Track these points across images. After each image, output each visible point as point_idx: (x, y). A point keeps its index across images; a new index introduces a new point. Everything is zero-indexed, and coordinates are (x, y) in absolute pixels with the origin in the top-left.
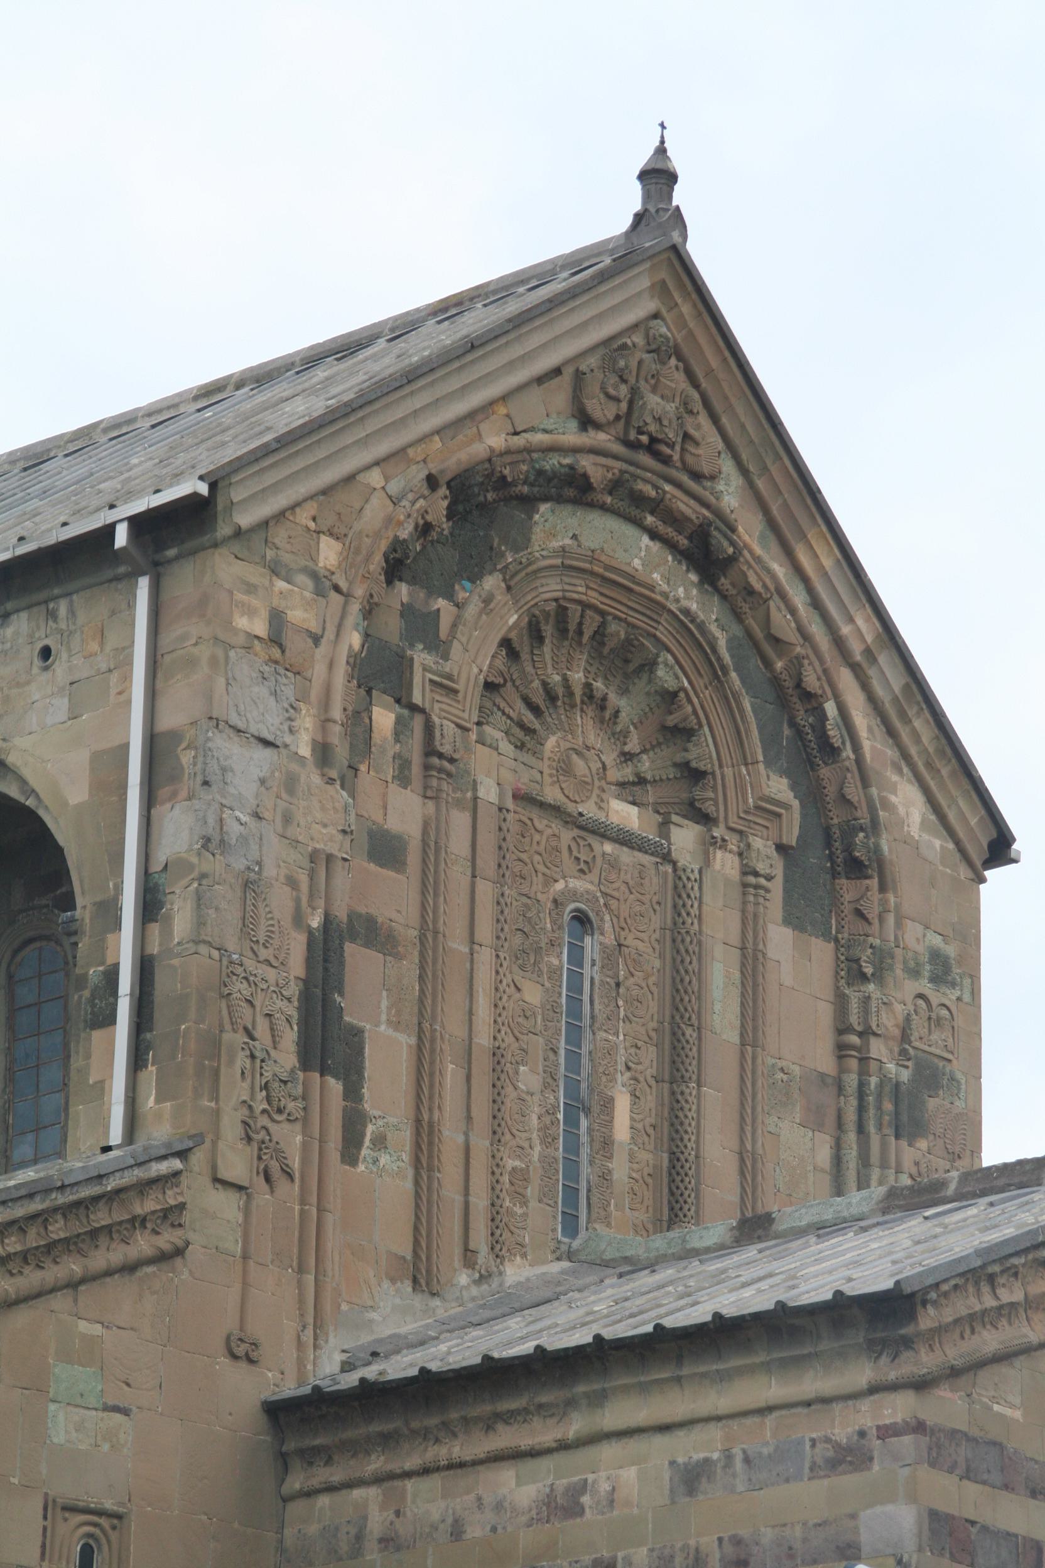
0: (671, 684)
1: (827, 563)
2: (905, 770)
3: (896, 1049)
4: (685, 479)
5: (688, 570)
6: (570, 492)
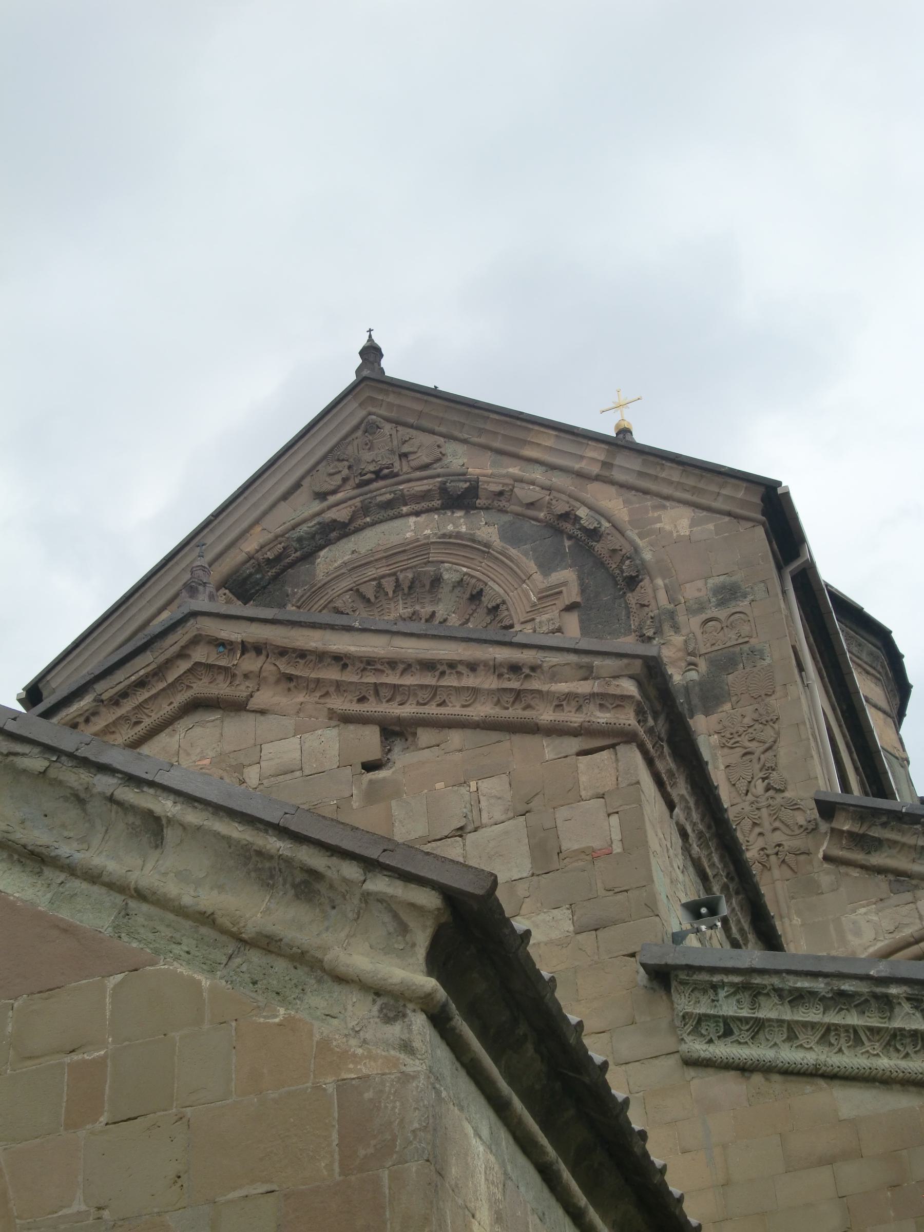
0: (455, 577)
1: (550, 443)
2: (667, 504)
3: (683, 664)
4: (418, 474)
5: (453, 513)
6: (333, 535)
